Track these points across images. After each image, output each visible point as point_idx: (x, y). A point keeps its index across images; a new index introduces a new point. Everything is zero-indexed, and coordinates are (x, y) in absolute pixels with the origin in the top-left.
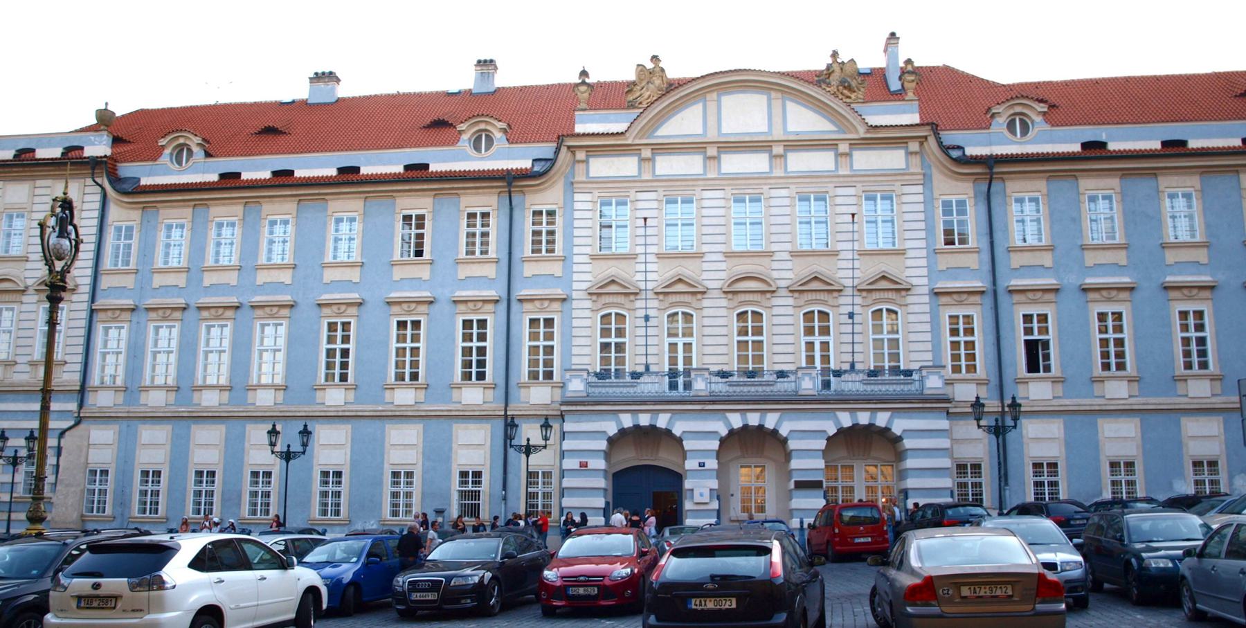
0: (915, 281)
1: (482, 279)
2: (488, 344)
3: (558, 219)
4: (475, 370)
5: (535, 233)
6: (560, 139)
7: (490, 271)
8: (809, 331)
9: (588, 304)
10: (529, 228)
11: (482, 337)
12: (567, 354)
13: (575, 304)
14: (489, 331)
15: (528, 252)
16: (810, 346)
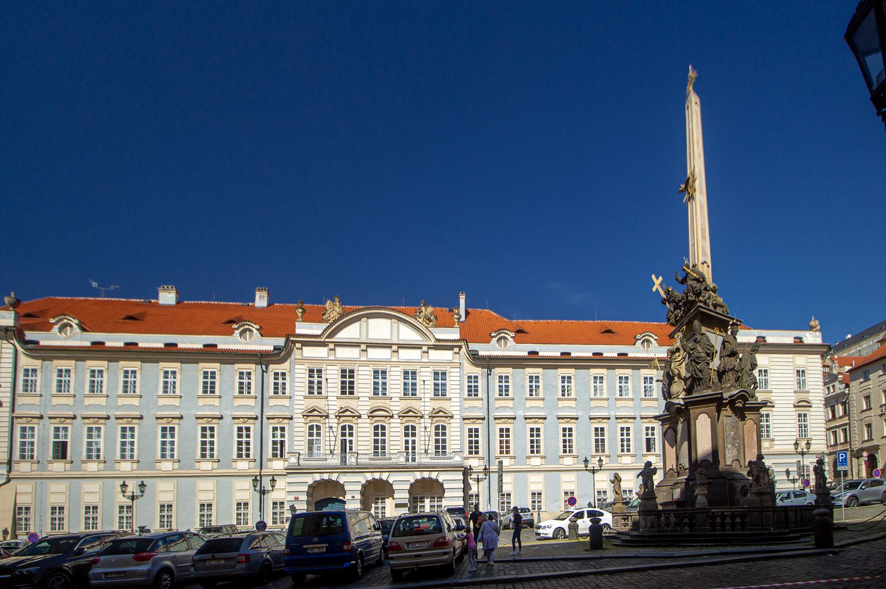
0: (454, 413)
1: (248, 406)
2: (251, 440)
3: (287, 377)
4: (243, 452)
5: (276, 384)
6: (287, 337)
7: (252, 402)
8: (406, 435)
9: (303, 420)
10: (272, 381)
11: (248, 436)
12: (292, 445)
13: (295, 420)
14: (252, 433)
15: (271, 393)
16: (407, 442)
